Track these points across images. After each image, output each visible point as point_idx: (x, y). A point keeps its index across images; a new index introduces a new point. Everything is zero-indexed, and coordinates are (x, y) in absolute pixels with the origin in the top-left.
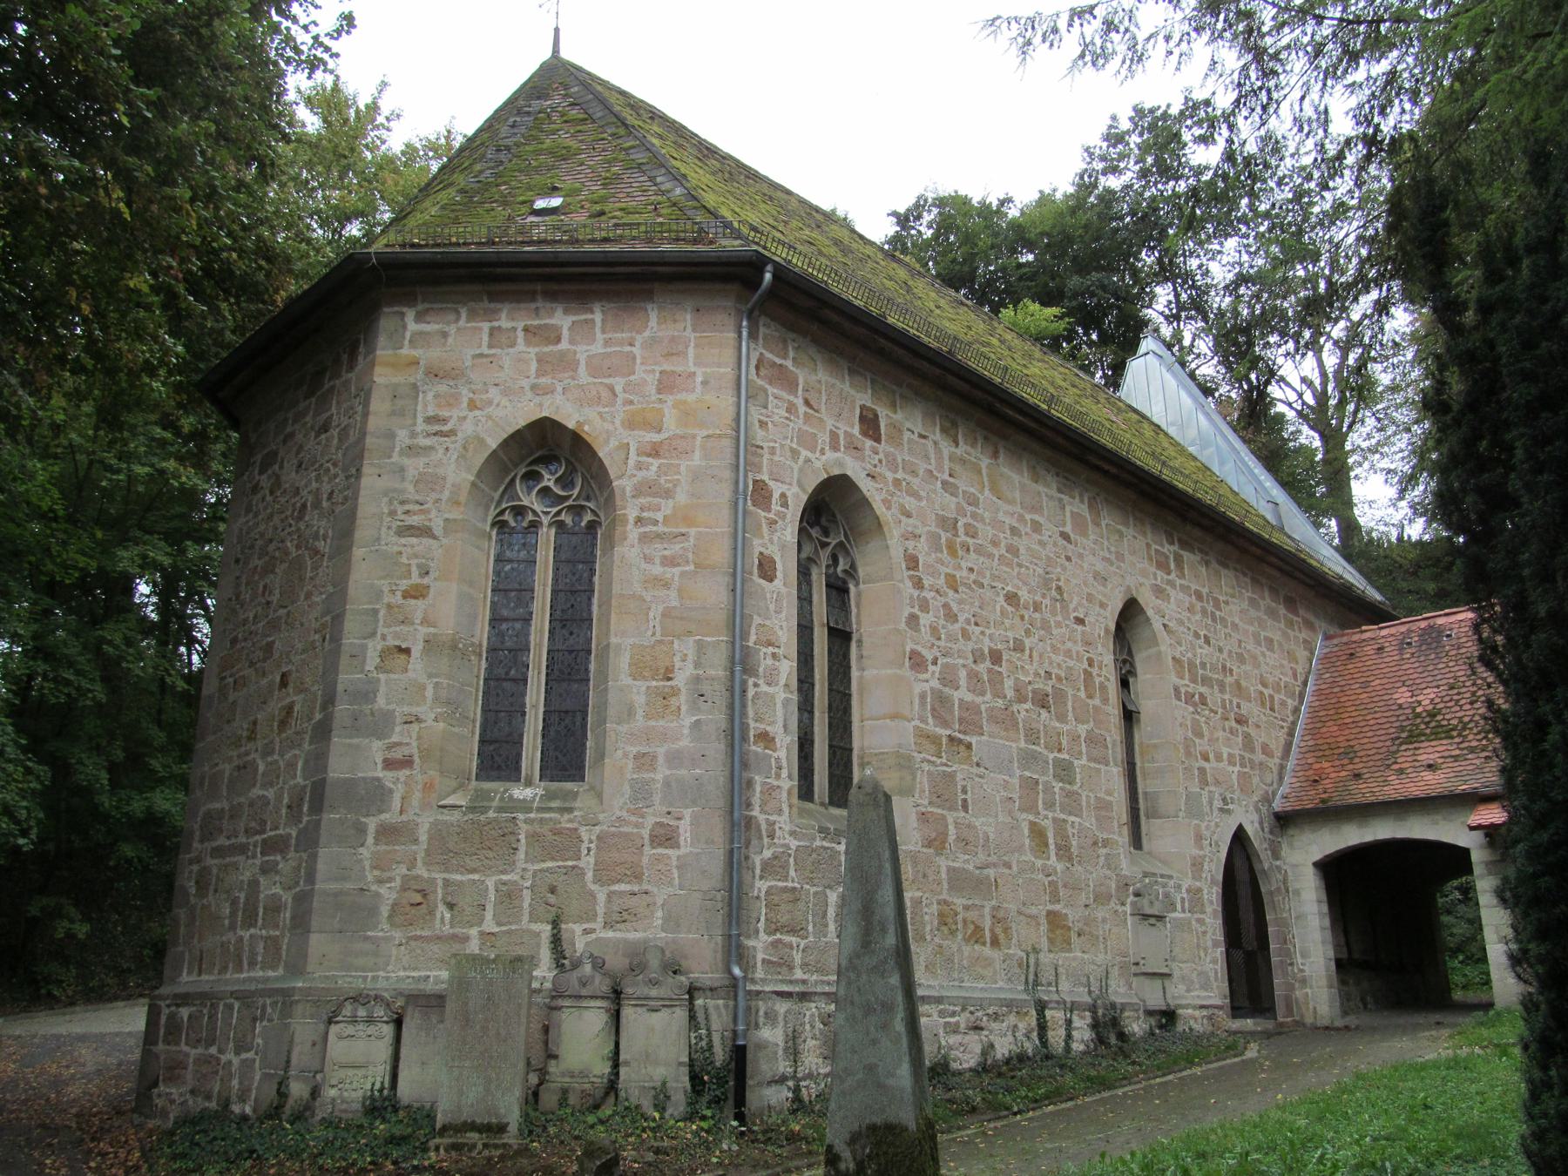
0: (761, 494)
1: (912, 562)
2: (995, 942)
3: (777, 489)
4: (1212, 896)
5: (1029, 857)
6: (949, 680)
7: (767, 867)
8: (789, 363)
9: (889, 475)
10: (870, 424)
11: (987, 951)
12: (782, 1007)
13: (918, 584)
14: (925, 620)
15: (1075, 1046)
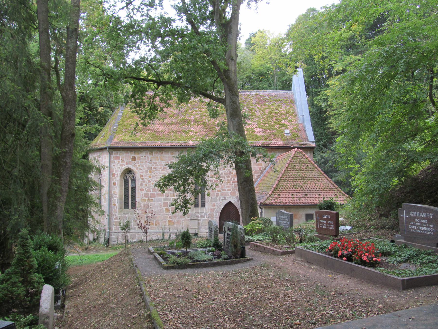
0: (114, 175)
1: (141, 176)
2: (156, 225)
3: (116, 173)
4: (169, 271)
5: (165, 213)
6: (149, 191)
7: (114, 219)
8: (119, 156)
9: (137, 165)
10: (134, 159)
11: (154, 226)
12: (115, 234)
13: (143, 179)
14: (144, 184)
15: (171, 238)
